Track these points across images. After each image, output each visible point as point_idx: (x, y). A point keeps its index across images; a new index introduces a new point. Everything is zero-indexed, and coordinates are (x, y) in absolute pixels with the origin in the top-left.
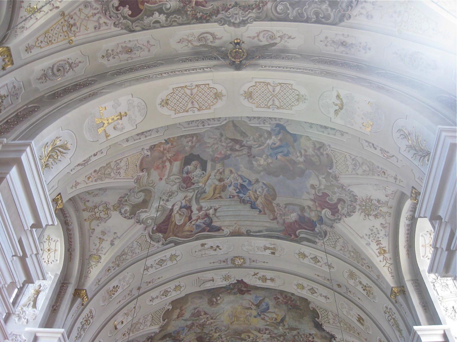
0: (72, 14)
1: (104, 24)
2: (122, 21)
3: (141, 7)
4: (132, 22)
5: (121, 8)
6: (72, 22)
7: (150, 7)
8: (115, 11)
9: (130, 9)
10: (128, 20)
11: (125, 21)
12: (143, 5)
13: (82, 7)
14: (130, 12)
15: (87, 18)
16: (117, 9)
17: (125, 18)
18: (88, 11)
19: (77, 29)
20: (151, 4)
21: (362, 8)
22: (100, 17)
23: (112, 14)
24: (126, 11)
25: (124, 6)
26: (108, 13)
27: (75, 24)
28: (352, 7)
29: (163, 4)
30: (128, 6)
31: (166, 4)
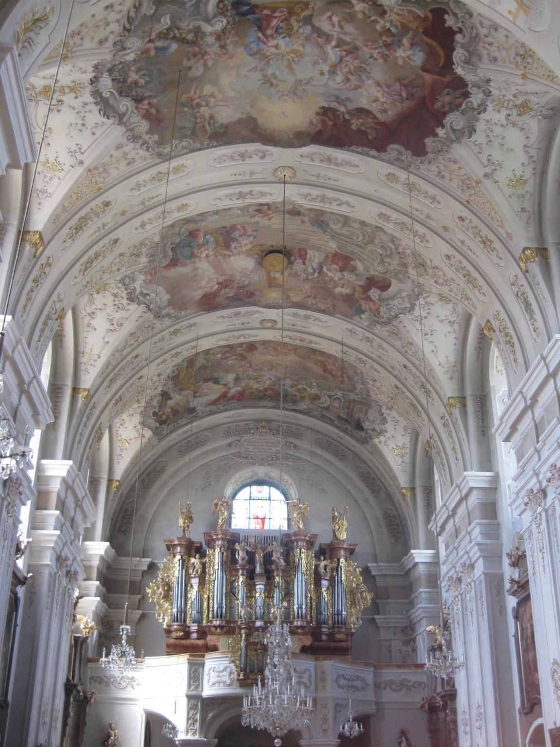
0: (514, 66)
1: (484, 26)
2: (460, 15)
3: (430, 15)
4: (447, 4)
5: (455, 28)
6: (519, 59)
7: (418, 9)
8: (464, 30)
9: (444, 21)
10: (451, 10)
11: (457, 11)
12: (426, 17)
13: (500, 62)
14: (446, 17)
15: (501, 47)
16: (460, 31)
17: (455, 15)
18: (496, 54)
19: (517, 47)
20: (415, 13)
21: (121, 11)
22: (486, 36)
23: (469, 30)
24: (450, 21)
25: (450, 28)
26: (474, 34)
27: (517, 54)
28: (135, 7)
29: (400, 5)
30: (446, 25)
31: (396, 4)
